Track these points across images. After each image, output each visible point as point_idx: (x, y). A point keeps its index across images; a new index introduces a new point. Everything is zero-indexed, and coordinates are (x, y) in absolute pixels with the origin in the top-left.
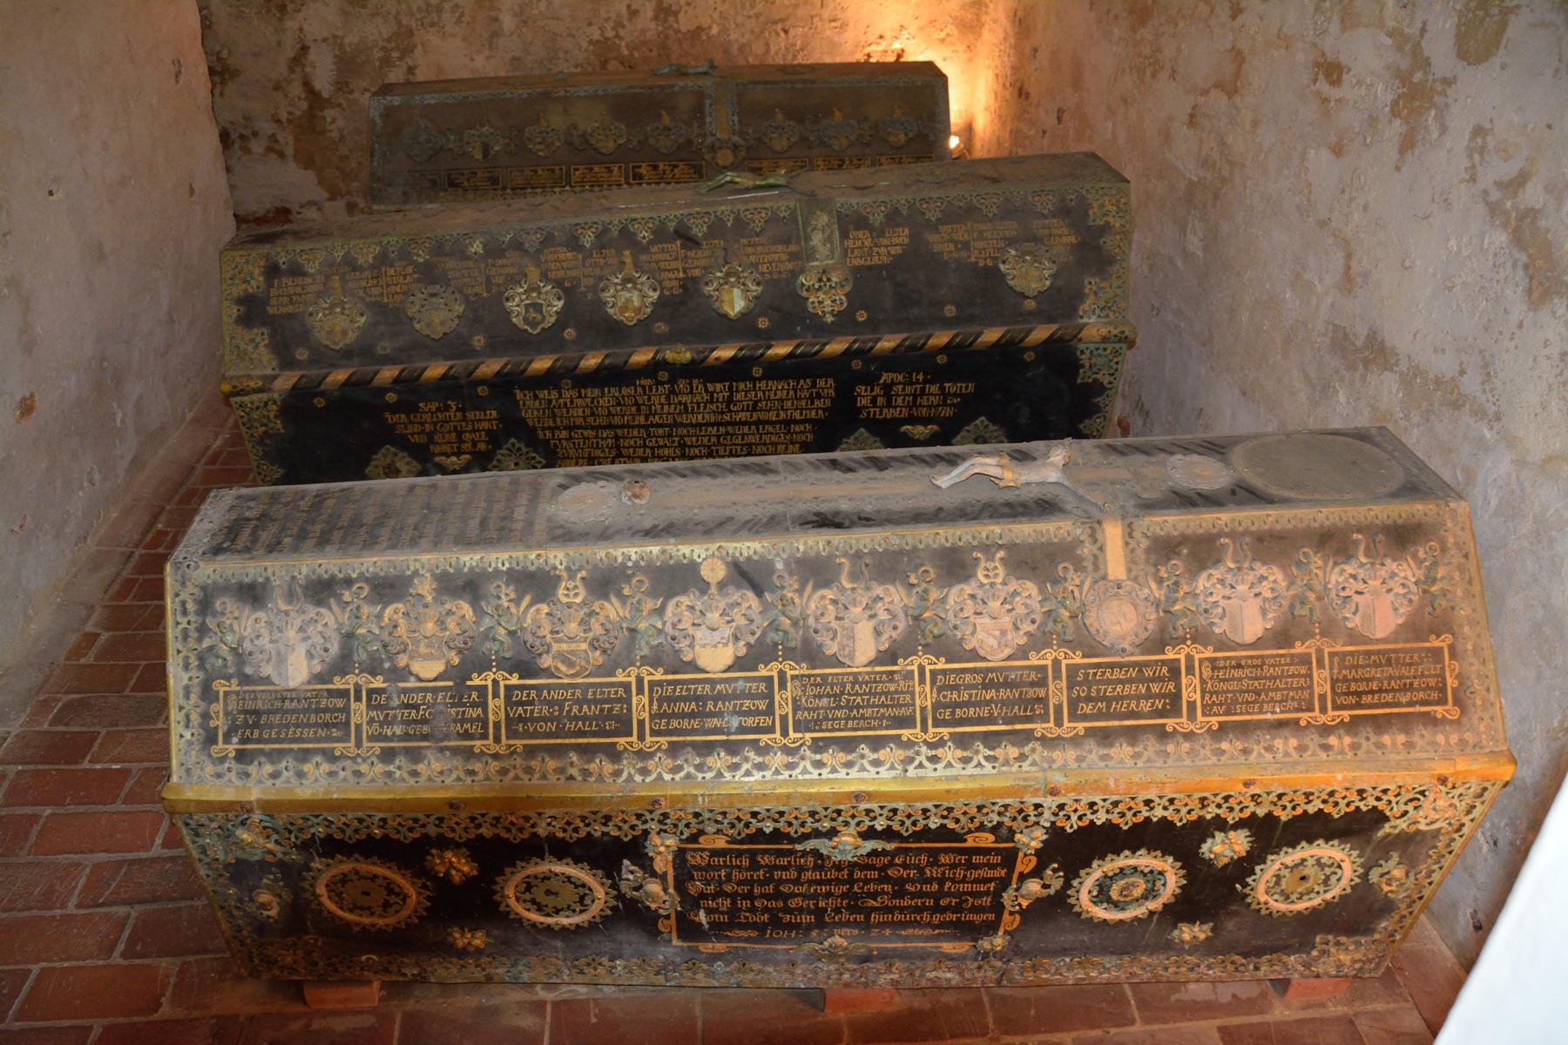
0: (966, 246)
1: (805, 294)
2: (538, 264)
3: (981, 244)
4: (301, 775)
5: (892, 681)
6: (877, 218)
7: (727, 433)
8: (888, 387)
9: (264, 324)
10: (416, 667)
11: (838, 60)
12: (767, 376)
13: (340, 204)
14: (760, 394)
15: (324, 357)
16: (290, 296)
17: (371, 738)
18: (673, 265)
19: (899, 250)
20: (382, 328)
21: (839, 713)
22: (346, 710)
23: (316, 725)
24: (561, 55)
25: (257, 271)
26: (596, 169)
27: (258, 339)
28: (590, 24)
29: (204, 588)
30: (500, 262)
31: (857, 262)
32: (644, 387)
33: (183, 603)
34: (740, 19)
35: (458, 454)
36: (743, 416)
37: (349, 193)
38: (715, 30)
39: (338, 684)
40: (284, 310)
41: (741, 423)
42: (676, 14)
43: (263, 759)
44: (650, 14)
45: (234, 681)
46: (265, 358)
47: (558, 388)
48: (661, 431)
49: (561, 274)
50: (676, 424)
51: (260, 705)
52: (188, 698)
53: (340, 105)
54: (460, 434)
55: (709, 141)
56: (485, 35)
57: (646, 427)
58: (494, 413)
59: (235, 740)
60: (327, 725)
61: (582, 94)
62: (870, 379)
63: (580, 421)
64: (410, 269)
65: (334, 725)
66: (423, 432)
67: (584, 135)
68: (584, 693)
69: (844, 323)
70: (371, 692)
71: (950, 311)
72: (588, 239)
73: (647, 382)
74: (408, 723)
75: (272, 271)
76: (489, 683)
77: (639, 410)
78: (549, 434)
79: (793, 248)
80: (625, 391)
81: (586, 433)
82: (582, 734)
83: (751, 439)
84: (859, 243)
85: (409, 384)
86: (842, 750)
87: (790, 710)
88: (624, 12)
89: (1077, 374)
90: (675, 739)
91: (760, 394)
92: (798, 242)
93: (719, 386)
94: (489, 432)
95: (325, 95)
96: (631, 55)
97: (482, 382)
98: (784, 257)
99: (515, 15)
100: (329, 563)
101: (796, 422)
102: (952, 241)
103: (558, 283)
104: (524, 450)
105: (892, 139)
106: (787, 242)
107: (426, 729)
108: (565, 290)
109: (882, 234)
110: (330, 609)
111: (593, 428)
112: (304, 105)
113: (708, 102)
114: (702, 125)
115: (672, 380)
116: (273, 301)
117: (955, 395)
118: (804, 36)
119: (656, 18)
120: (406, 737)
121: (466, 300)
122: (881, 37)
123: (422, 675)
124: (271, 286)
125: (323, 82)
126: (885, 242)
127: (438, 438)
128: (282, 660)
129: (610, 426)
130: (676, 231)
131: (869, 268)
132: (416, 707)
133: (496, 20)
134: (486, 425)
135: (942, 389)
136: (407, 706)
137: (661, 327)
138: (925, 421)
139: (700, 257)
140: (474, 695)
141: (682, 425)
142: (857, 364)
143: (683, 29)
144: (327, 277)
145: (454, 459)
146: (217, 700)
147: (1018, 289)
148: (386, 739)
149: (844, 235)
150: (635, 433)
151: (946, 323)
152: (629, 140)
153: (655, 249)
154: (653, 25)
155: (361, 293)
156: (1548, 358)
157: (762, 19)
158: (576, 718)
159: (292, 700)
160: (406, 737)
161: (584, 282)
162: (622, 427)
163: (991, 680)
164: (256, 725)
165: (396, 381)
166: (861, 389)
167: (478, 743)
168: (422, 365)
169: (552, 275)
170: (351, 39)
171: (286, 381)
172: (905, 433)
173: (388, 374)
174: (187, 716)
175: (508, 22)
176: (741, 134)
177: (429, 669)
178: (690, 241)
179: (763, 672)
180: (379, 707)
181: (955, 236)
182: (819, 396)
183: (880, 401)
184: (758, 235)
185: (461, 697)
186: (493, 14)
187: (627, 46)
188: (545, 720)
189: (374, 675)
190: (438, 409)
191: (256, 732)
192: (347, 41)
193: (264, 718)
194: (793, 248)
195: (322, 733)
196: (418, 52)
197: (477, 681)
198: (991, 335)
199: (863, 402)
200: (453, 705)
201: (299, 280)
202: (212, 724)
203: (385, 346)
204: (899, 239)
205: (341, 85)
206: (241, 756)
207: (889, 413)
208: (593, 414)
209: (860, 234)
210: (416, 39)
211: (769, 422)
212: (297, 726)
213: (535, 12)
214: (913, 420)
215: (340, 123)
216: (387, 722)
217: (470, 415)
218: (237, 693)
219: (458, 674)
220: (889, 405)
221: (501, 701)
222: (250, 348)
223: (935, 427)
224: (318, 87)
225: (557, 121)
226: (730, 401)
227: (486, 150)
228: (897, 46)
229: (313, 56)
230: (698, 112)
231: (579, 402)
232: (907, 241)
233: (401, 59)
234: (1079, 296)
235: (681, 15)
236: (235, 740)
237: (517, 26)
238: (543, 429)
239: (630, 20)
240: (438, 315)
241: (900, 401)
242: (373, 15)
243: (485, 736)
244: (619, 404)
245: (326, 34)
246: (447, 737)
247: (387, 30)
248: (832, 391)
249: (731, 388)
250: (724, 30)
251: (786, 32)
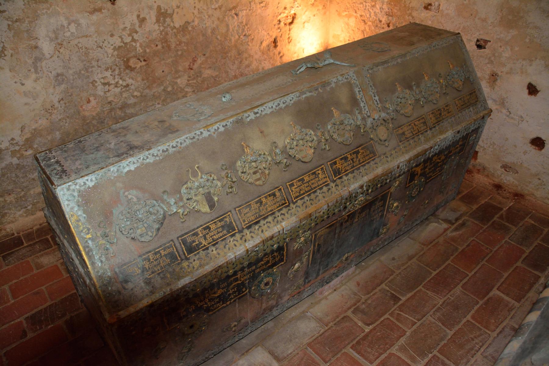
24: (94, 63)
28: (112, 35)
34: (210, 12)
42: (171, 16)
44: (154, 19)
56: (30, 61)
61: (268, 111)
67: (284, 151)
88: (136, 21)
96: (145, 51)
99: (51, 40)
113: (357, 90)
118: (247, 15)
119: (158, 21)
122: (285, 8)
133: (36, 47)
143: (177, 26)
152: (319, 142)
154: (156, 27)
157: (223, 9)
175: (46, 47)
176: (385, 109)
186: (33, 43)
187: (141, 46)
213: (68, 34)
225: (258, 145)
227: (209, 199)
228: (293, 12)
230: (354, 102)
235: (175, 16)
237: (55, 48)
239: (140, 26)
251: (237, 15)
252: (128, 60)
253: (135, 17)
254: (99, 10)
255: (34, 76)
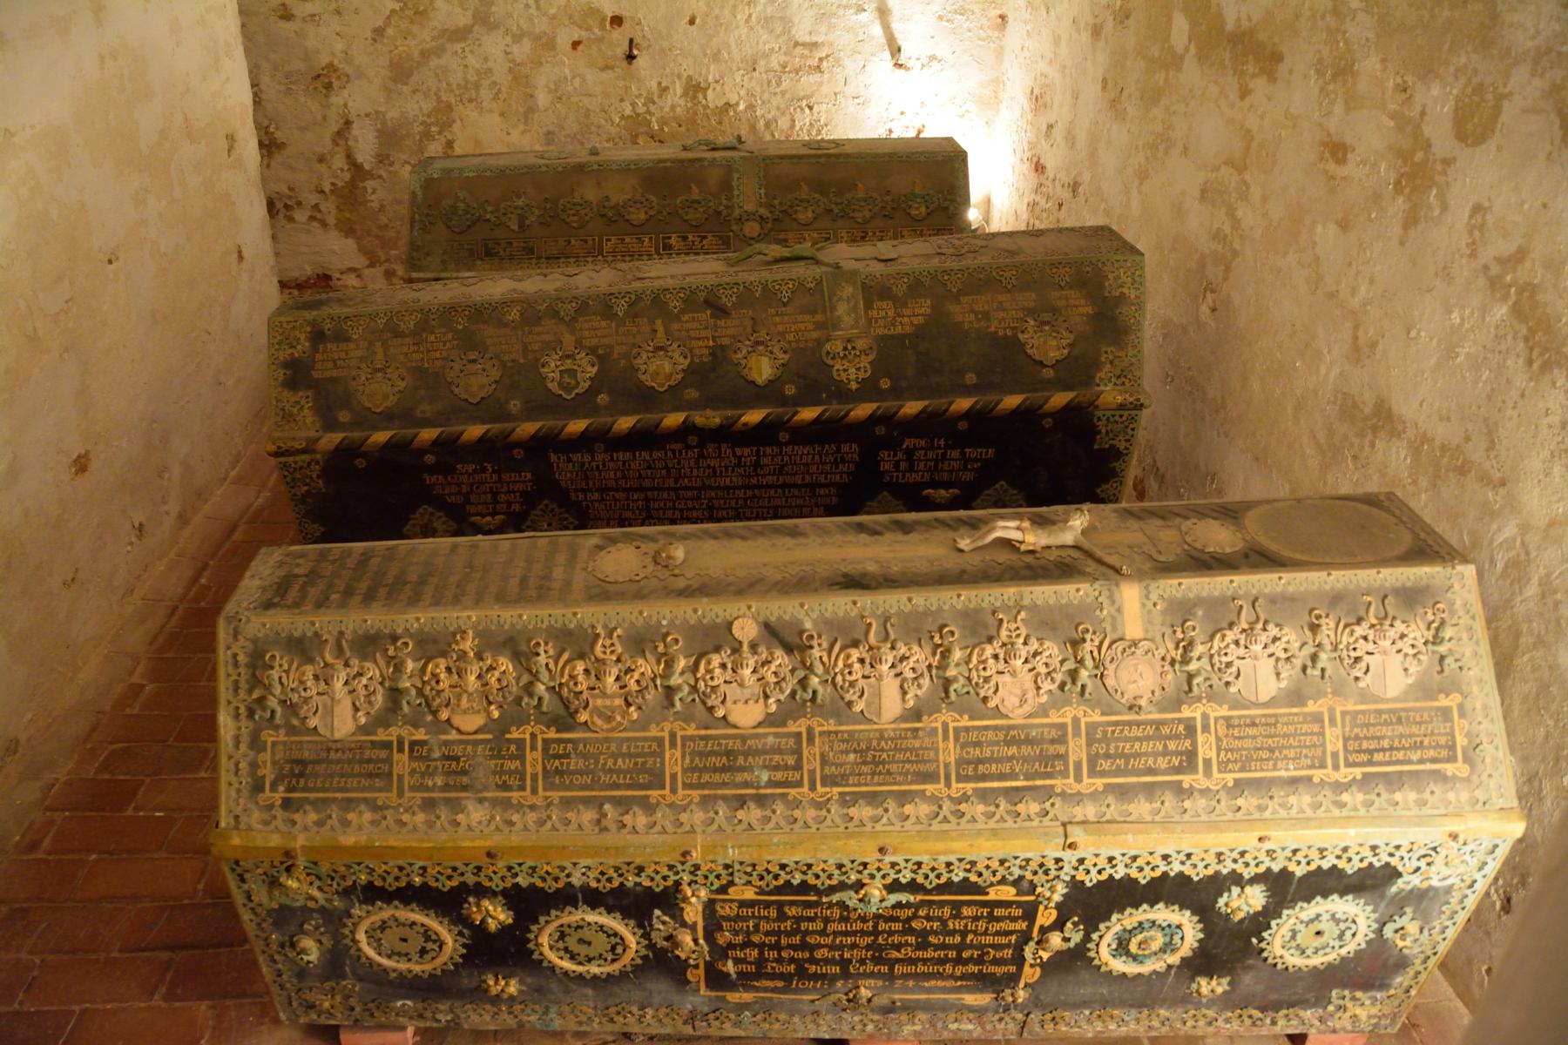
0: (986, 316)
1: (830, 362)
2: (573, 331)
3: (1001, 315)
4: (345, 823)
5: (915, 737)
6: (900, 290)
7: (754, 496)
8: (910, 452)
9: (309, 387)
10: (456, 721)
11: (861, 136)
12: (792, 442)
13: (378, 272)
14: (786, 459)
15: (367, 420)
16: (334, 361)
17: (413, 789)
18: (703, 334)
19: (921, 320)
20: (422, 393)
21: (865, 769)
22: (389, 761)
23: (360, 775)
24: (594, 129)
25: (302, 337)
26: (628, 240)
27: (303, 402)
28: (622, 100)
29: (255, 641)
30: (536, 330)
31: (881, 331)
32: (673, 451)
33: (235, 656)
34: (766, 96)
35: (493, 515)
36: (770, 479)
37: (387, 260)
38: (742, 107)
39: (381, 735)
40: (328, 374)
41: (768, 486)
42: (705, 90)
43: (308, 808)
44: (679, 91)
45: (282, 731)
46: (309, 420)
47: (591, 452)
48: (689, 494)
49: (594, 342)
50: (704, 487)
51: (306, 754)
52: (237, 746)
53: (380, 177)
54: (495, 495)
55: (737, 212)
57: (676, 490)
58: (529, 476)
59: (281, 788)
60: (370, 775)
62: (893, 446)
63: (612, 484)
64: (450, 336)
65: (377, 775)
66: (459, 493)
68: (620, 747)
69: (868, 390)
70: (413, 744)
71: (971, 378)
72: (621, 308)
73: (676, 446)
74: (448, 774)
75: (318, 336)
76: (527, 736)
77: (669, 472)
78: (581, 496)
79: (819, 317)
80: (656, 454)
81: (617, 495)
82: (616, 786)
83: (777, 502)
84: (882, 313)
85: (448, 447)
86: (869, 804)
87: (818, 764)
89: (1094, 440)
90: (706, 792)
91: (786, 459)
92: (824, 312)
93: (746, 451)
94: (523, 493)
95: (367, 167)
97: (518, 444)
98: (810, 326)
99: (550, 92)
100: (375, 619)
101: (821, 485)
102: (972, 311)
103: (593, 351)
104: (557, 510)
105: (914, 212)
106: (813, 312)
107: (465, 780)
108: (600, 357)
109: (905, 305)
110: (376, 662)
111: (624, 490)
112: (347, 176)
113: (736, 176)
114: (729, 198)
115: (701, 445)
116: (318, 366)
117: (976, 460)
119: (685, 94)
120: (446, 787)
121: (503, 364)
123: (464, 728)
124: (316, 350)
125: (365, 156)
126: (906, 312)
127: (473, 498)
128: (330, 712)
129: (641, 489)
130: (706, 302)
131: (892, 337)
132: (457, 759)
134: (521, 487)
135: (963, 453)
136: (448, 758)
137: (692, 394)
138: (946, 485)
139: (729, 328)
140: (513, 748)
141: (711, 488)
142: (880, 430)
144: (371, 343)
145: (489, 518)
146: (264, 749)
147: (1037, 358)
148: (427, 789)
149: (869, 306)
150: (665, 495)
151: (967, 391)
152: (660, 212)
153: (686, 317)
154: (682, 102)
155: (402, 358)
156: (1550, 427)
157: (788, 96)
158: (611, 771)
159: (337, 750)
160: (446, 787)
161: (618, 350)
162: (652, 489)
163: (1012, 736)
164: (302, 774)
165: (435, 443)
166: (884, 454)
167: (515, 794)
168: (461, 428)
169: (586, 343)
170: (393, 114)
171: (331, 440)
172: (927, 497)
173: (428, 435)
174: (237, 765)
175: (543, 99)
177: (470, 722)
178: (720, 311)
179: (792, 728)
180: (421, 758)
181: (976, 307)
182: (843, 460)
183: (903, 465)
184: (785, 305)
185: (500, 751)
188: (581, 773)
189: (416, 726)
190: (475, 471)
191: (302, 782)
192: (389, 115)
193: (309, 768)
194: (819, 317)
195: (365, 782)
196: (456, 127)
197: (515, 735)
198: (1012, 401)
199: (886, 467)
200: (492, 757)
201: (343, 346)
202: (260, 773)
203: (425, 409)
204: (924, 307)
205: (382, 159)
206: (287, 804)
207: (912, 478)
208: (624, 477)
209: (884, 304)
210: (455, 115)
211: (794, 486)
212: (342, 776)
213: (570, 88)
214: (934, 484)
215: (381, 194)
216: (428, 773)
217: (505, 477)
218: (284, 743)
219: (499, 729)
220: (911, 470)
221: (538, 754)
222: (295, 411)
223: (956, 491)
224: (360, 159)
226: (757, 464)
227: (522, 220)
229: (356, 130)
230: (726, 186)
231: (611, 464)
232: (929, 311)
233: (440, 133)
234: (1096, 365)
235: (710, 92)
236: (281, 788)
238: (576, 490)
239: (660, 97)
240: (478, 381)
241: (922, 465)
242: (414, 91)
243: (522, 788)
244: (649, 467)
245: (369, 110)
246: (485, 788)
247: (427, 105)
248: (856, 456)
249: (758, 451)
250: (751, 107)
251: (811, 108)
252: (636, 136)
253: (654, 84)
254: (612, 68)
255: (522, 127)
